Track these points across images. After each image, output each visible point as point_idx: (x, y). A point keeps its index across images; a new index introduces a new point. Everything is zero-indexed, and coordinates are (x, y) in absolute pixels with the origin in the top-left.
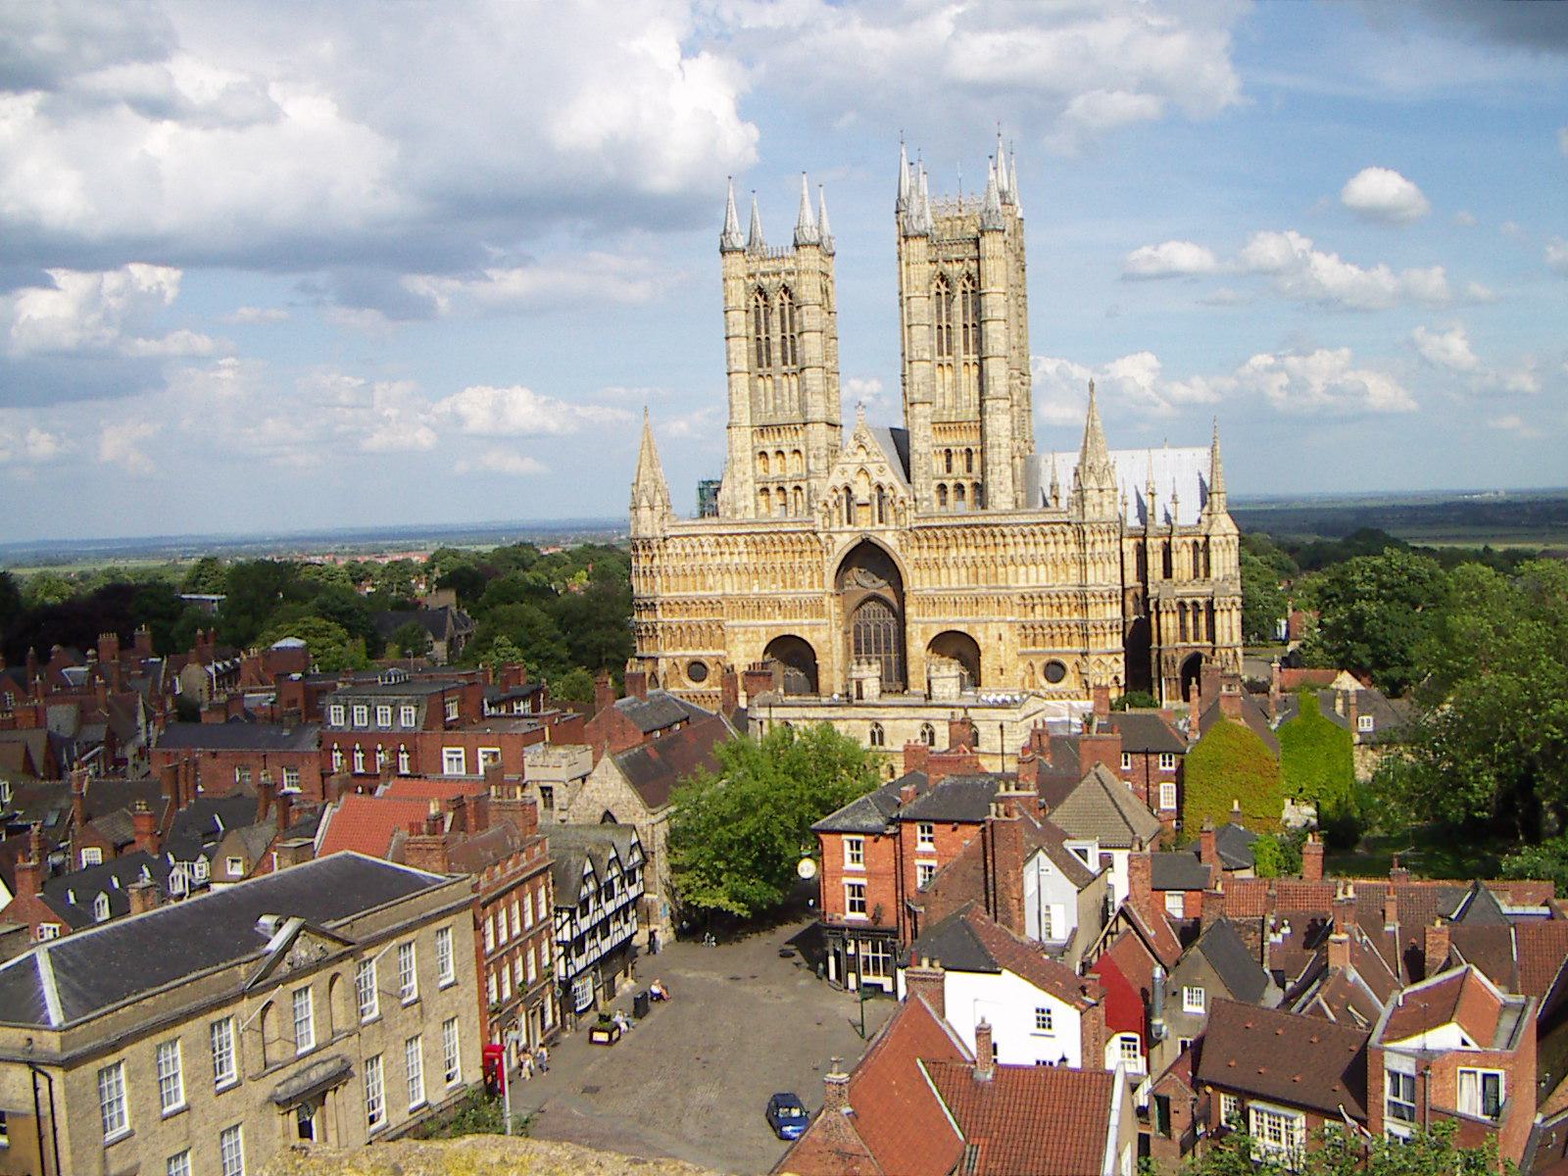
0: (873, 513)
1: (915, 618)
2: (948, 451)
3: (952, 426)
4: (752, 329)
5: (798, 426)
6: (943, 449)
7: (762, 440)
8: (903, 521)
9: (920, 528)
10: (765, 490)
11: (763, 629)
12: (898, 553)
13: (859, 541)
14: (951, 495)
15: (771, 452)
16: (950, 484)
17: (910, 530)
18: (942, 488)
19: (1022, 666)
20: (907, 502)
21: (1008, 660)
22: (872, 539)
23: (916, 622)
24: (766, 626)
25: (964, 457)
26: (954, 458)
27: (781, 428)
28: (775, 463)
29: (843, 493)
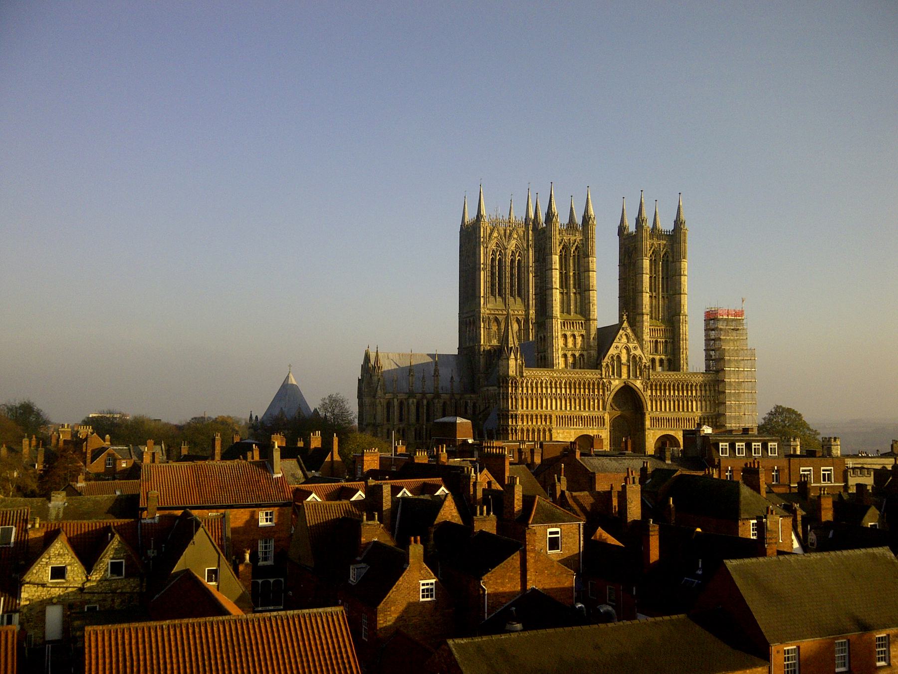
2: (656, 341)
3: (658, 328)
5: (583, 322)
6: (654, 340)
7: (563, 327)
10: (565, 356)
11: (573, 431)
12: (642, 392)
14: (657, 364)
15: (569, 334)
16: (657, 358)
18: (653, 360)
20: (647, 365)
22: (630, 383)
23: (649, 429)
24: (574, 429)
26: (659, 344)
27: (574, 321)
28: (570, 341)
29: (615, 358)
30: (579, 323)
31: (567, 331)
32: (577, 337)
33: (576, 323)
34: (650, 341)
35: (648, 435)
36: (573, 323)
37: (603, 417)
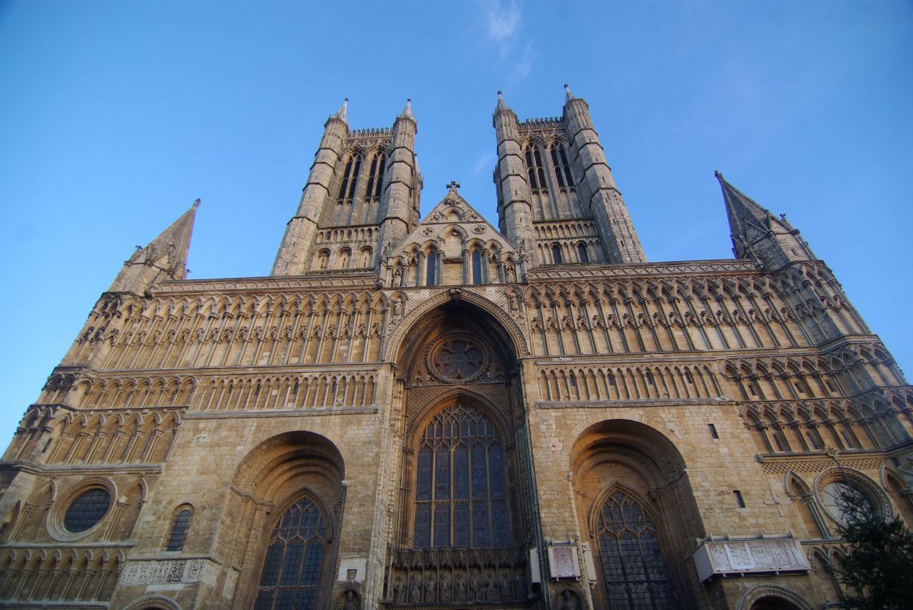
0: (465, 272)
1: (542, 400)
3: (558, 225)
4: (341, 173)
5: (373, 228)
8: (511, 278)
9: (540, 282)
11: (252, 424)
12: (507, 311)
13: (444, 299)
15: (335, 248)
17: (525, 283)
19: (777, 484)
20: (516, 257)
21: (744, 474)
24: (259, 416)
25: (577, 249)
26: (564, 249)
30: (363, 230)
31: (331, 243)
32: (352, 251)
33: (356, 231)
34: (540, 245)
35: (538, 428)
36: (350, 233)
37: (372, 377)
